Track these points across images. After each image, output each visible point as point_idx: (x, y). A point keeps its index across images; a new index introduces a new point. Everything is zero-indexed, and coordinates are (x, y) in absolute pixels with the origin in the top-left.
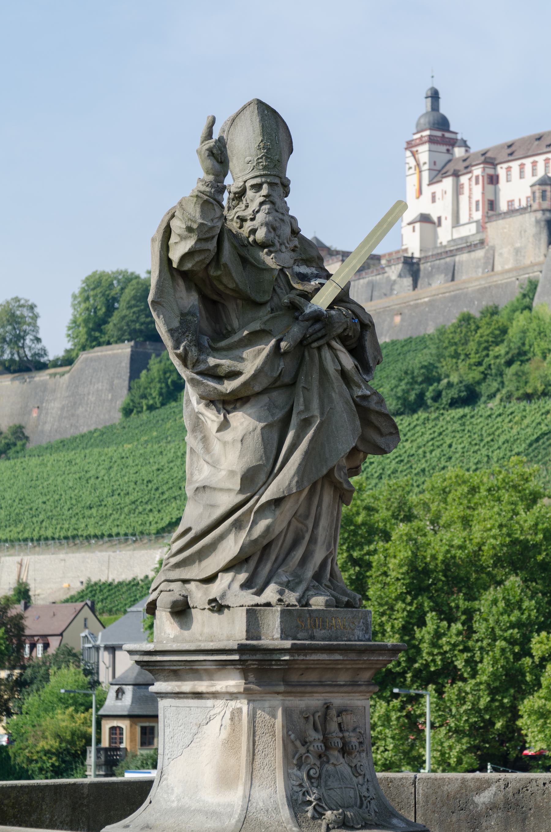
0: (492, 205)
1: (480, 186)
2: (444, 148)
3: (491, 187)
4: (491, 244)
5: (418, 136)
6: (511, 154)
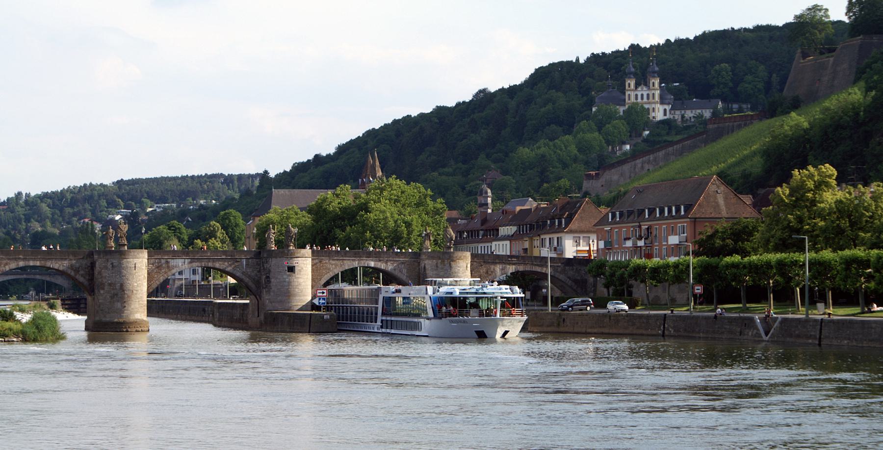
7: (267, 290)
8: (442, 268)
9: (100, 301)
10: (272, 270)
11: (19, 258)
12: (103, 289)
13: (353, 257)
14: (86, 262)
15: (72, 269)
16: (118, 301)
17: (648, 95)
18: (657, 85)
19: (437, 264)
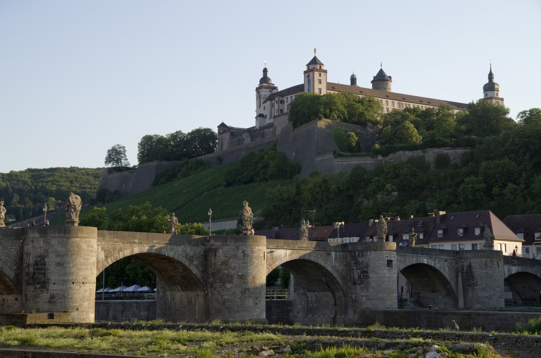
0: (282, 111)
1: (277, 104)
2: (268, 90)
3: (281, 105)
4: (275, 126)
5: (260, 85)
6: (288, 93)
9: (226, 297)
10: (370, 264)
11: (135, 243)
12: (231, 282)
13: (412, 253)
14: (199, 250)
15: (186, 258)
16: (250, 297)
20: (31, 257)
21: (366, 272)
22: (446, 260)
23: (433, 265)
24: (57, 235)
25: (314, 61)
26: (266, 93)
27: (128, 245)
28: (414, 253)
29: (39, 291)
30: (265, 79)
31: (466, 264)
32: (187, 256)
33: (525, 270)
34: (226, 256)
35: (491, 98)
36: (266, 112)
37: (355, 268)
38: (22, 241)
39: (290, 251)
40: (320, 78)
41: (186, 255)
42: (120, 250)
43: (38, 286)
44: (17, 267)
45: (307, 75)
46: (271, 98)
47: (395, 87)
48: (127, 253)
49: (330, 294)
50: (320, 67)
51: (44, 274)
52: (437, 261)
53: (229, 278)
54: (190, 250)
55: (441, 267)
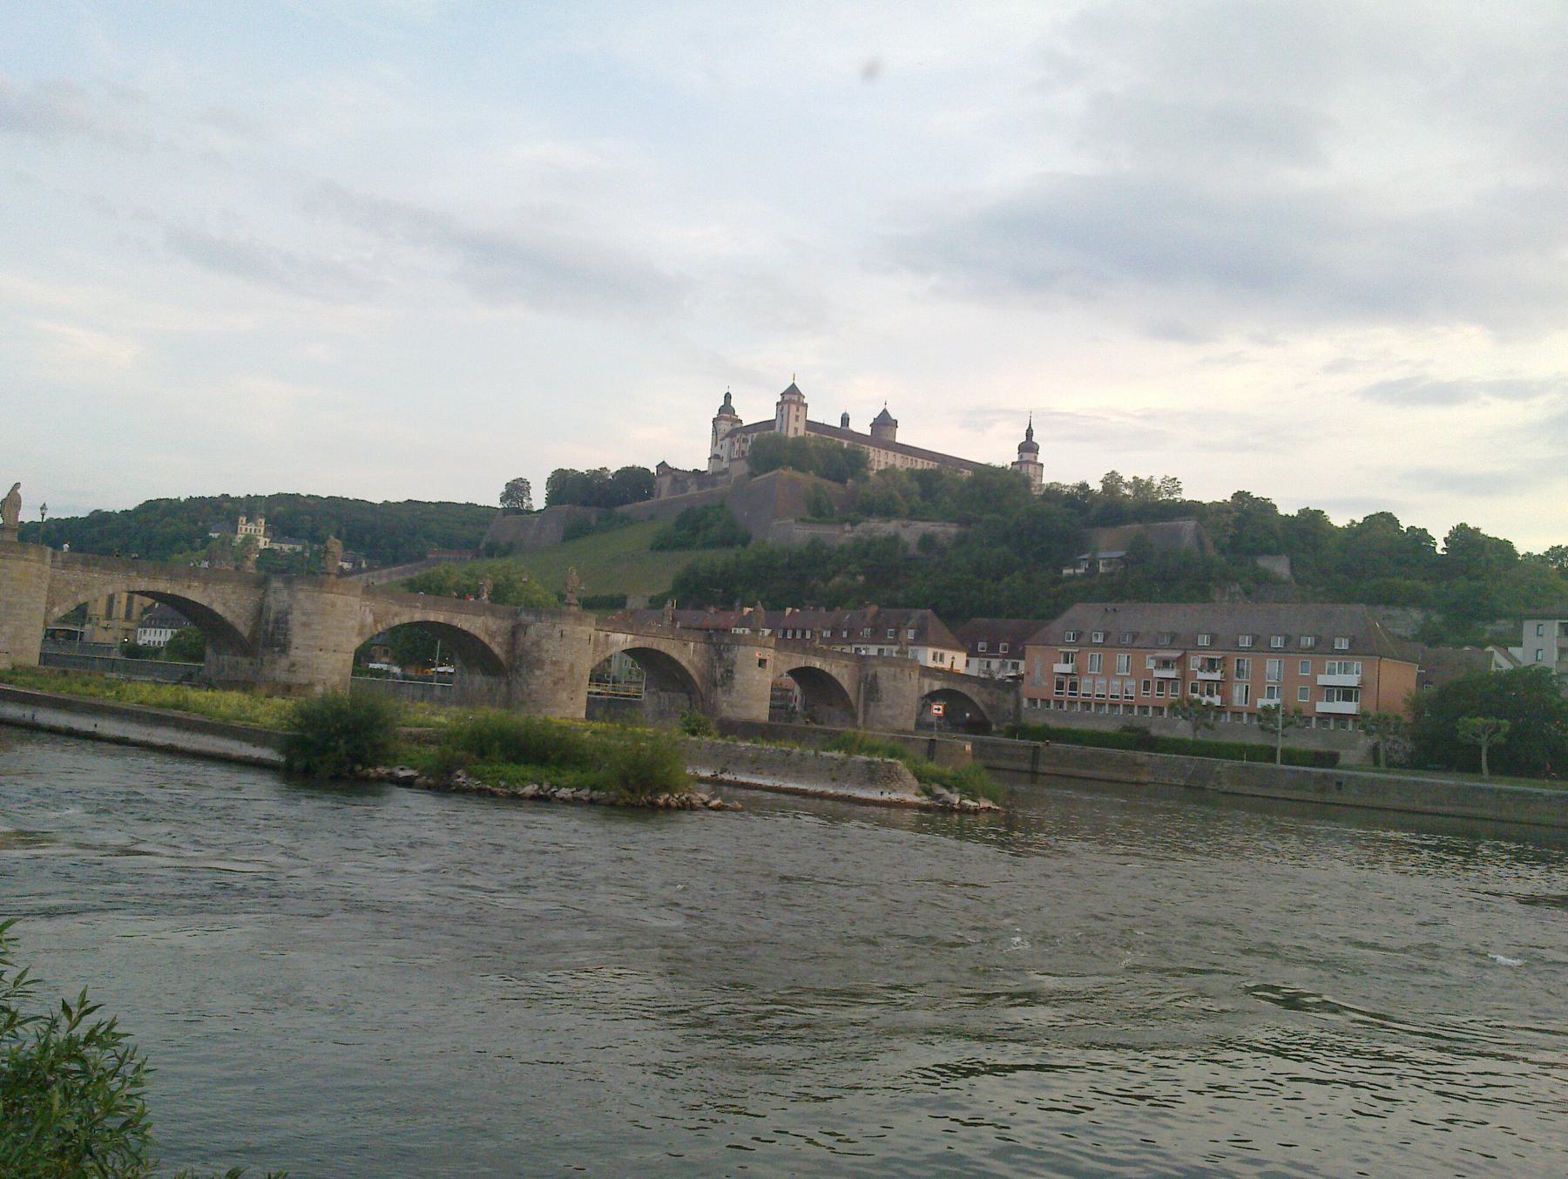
3: (742, 444)
7: (725, 688)
8: (900, 679)
9: (534, 687)
11: (416, 607)
14: (507, 624)
15: (487, 633)
17: (255, 530)
18: (263, 523)
19: (895, 672)
20: (272, 612)
21: (731, 672)
22: (846, 666)
23: (827, 670)
24: (306, 587)
25: (793, 389)
26: (725, 427)
27: (408, 609)
28: (803, 654)
29: (276, 656)
30: (726, 409)
31: (871, 672)
32: (487, 631)
33: (950, 687)
34: (538, 635)
35: (1028, 462)
36: (723, 453)
37: (718, 665)
38: (263, 591)
39: (632, 636)
40: (798, 414)
41: (487, 630)
42: (396, 615)
43: (277, 649)
44: (254, 624)
45: (780, 407)
46: (731, 434)
47: (901, 437)
48: (405, 619)
49: (685, 696)
50: (799, 399)
51: (286, 635)
52: (833, 666)
53: (540, 663)
54: (493, 623)
55: (838, 674)
